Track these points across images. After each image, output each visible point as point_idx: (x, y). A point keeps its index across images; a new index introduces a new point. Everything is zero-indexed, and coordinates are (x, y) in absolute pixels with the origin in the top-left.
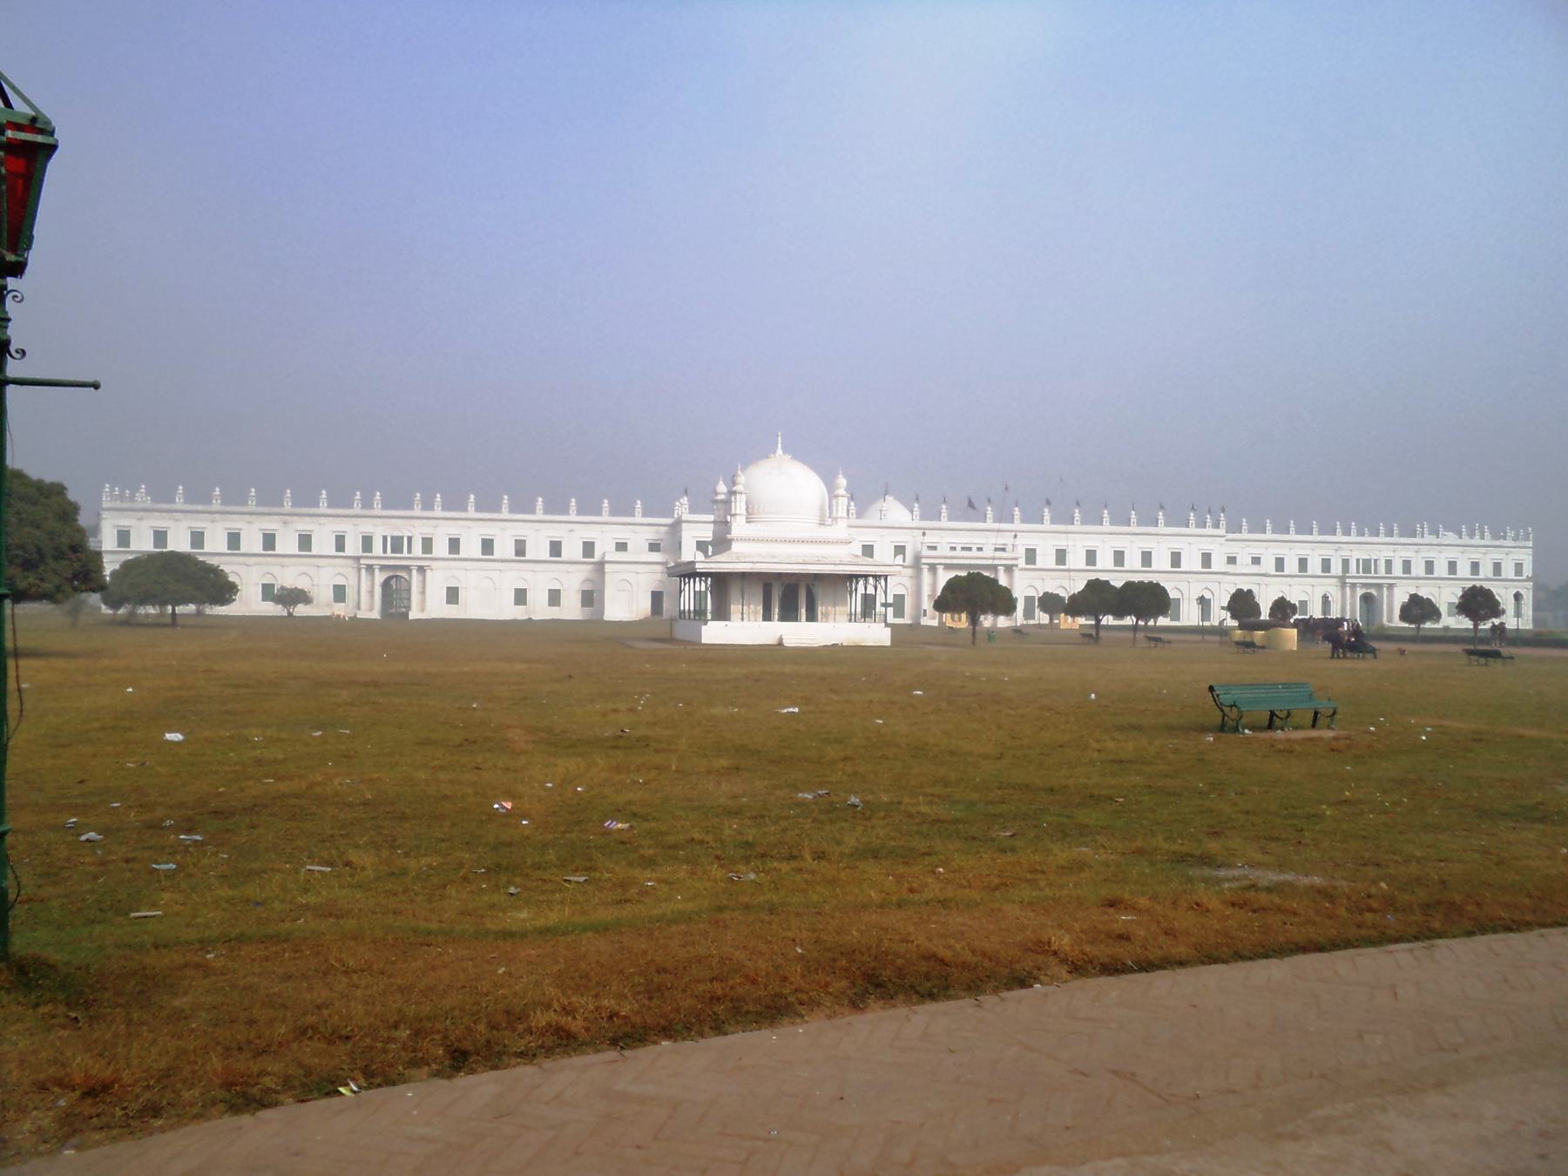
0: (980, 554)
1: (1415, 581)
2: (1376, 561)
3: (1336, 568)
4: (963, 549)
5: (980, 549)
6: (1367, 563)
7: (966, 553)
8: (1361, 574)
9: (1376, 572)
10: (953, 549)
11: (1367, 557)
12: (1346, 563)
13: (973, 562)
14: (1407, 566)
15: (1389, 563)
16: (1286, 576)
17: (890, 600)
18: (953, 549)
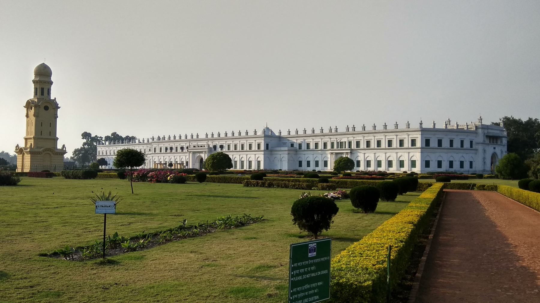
0: (194, 148)
1: (385, 150)
2: (345, 142)
3: (329, 146)
4: (202, 146)
5: (204, 146)
6: (341, 143)
7: (200, 148)
8: (339, 149)
9: (345, 148)
10: (194, 147)
11: (341, 141)
12: (332, 144)
13: (198, 150)
14: (358, 144)
15: (350, 143)
16: (431, 148)
17: (108, 165)
18: (194, 147)
